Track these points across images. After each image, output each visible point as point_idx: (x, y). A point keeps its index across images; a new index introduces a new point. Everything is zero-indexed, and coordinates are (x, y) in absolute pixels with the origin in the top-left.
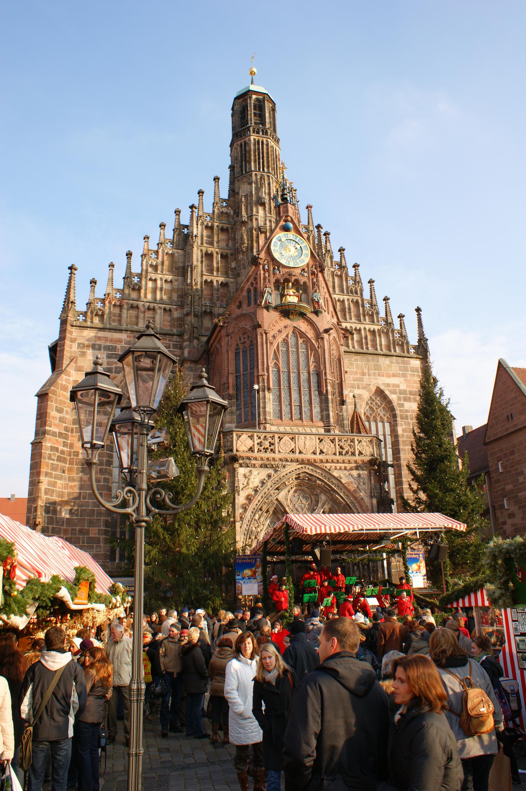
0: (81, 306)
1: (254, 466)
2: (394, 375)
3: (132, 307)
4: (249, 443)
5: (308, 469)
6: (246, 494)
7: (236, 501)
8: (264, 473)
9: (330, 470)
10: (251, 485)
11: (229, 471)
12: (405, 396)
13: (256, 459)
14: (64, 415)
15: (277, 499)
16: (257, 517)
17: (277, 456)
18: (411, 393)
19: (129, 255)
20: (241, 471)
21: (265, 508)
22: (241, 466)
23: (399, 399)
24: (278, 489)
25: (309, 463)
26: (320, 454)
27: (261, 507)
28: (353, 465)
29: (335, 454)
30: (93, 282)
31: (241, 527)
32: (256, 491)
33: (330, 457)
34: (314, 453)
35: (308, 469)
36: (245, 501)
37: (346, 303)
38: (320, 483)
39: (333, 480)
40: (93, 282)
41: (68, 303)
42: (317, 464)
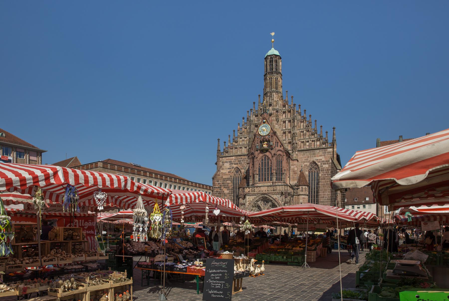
0: (222, 151)
2: (320, 156)
3: (236, 148)
4: (249, 190)
12: (324, 163)
14: (219, 182)
17: (256, 193)
18: (326, 161)
19: (234, 131)
20: (247, 197)
23: (321, 164)
25: (264, 194)
30: (225, 142)
37: (305, 132)
40: (225, 142)
41: (219, 151)
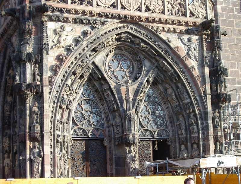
1: (67, 21)
5: (131, 29)
6: (57, 54)
7: (45, 61)
8: (79, 30)
9: (157, 31)
10: (63, 44)
11: (35, 25)
13: (69, 11)
15: (93, 63)
16: (69, 82)
17: (95, 9)
20: (51, 26)
21: (79, 72)
22: (51, 19)
24: (94, 50)
25: (133, 21)
26: (146, 11)
27: (75, 71)
28: (184, 28)
29: (163, 13)
31: (50, 93)
32: (68, 50)
33: (158, 16)
34: (139, 9)
35: (131, 29)
36: (54, 63)
38: (145, 46)
39: (160, 43)
42: (142, 23)
